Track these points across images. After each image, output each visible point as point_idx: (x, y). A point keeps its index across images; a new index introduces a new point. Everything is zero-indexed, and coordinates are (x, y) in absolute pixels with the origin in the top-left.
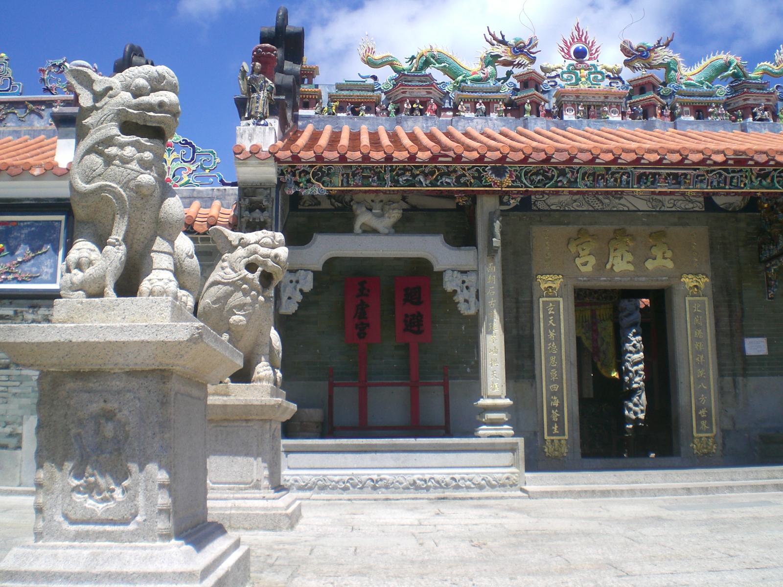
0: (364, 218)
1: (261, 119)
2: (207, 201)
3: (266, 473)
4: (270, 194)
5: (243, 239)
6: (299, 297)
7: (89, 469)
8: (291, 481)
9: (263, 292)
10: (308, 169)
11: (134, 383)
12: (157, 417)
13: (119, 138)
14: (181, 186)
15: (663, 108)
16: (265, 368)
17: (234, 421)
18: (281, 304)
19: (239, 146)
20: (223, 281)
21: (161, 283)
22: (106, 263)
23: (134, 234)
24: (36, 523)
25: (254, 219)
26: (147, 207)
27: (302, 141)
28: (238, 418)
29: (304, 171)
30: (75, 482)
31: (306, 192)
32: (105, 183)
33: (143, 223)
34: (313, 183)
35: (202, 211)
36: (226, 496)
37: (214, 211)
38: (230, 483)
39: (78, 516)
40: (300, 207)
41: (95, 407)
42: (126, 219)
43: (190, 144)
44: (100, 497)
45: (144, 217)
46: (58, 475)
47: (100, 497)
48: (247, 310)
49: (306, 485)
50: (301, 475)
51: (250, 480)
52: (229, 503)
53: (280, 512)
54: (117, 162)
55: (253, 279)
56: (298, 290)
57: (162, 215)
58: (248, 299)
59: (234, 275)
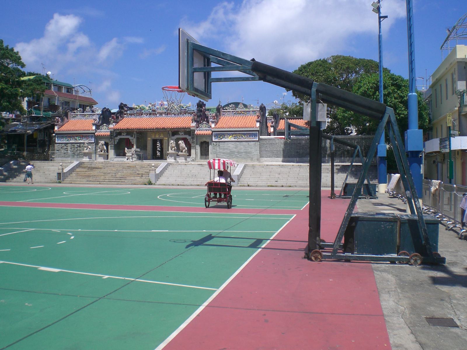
0: (122, 134)
15: (170, 114)
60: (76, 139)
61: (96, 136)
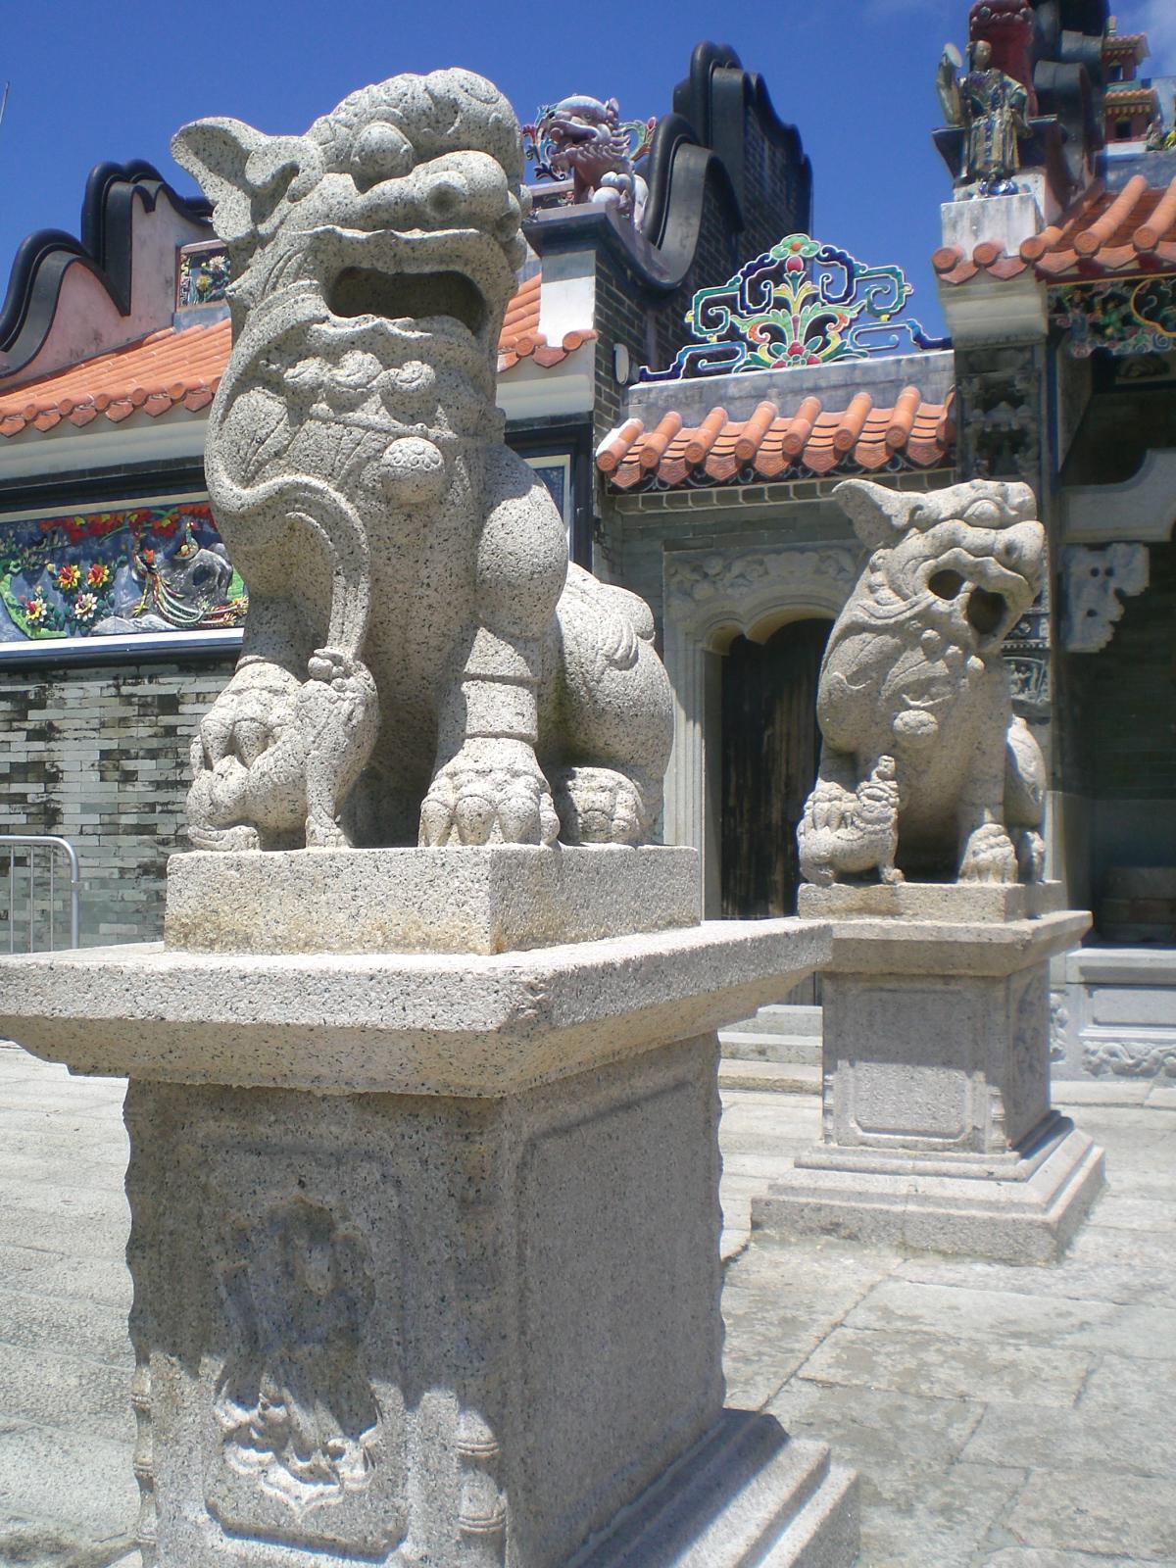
1: (999, 179)
2: (886, 390)
3: (997, 1110)
4: (1031, 362)
5: (920, 508)
6: (1114, 611)
7: (268, 1385)
8: (1101, 1054)
9: (980, 644)
10: (1124, 291)
11: (380, 1134)
12: (450, 1245)
13: (324, 327)
14: (825, 360)
16: (993, 840)
17: (913, 977)
18: (1070, 630)
19: (949, 250)
20: (873, 621)
21: (481, 786)
22: (304, 738)
23: (404, 629)
24: (142, 1517)
25: (996, 426)
26: (432, 540)
27: (1106, 223)
28: (923, 971)
29: (1112, 297)
30: (240, 1415)
31: (1127, 348)
32: (305, 479)
33: (421, 591)
34: (1138, 326)
35: (877, 415)
36: (895, 1163)
37: (900, 415)
38: (905, 1132)
39: (244, 1517)
40: (1119, 381)
41: (279, 1197)
42: (364, 586)
43: (840, 258)
44: (305, 1465)
45: (424, 573)
46: (188, 1387)
47: (305, 1465)
48: (938, 695)
49: (1137, 1065)
50: (1125, 1039)
51: (955, 1127)
52: (903, 1185)
53: (1029, 1216)
54: (321, 407)
55: (950, 615)
56: (1111, 592)
57: (485, 558)
58: (940, 668)
59: (901, 605)
60: (203, 574)
61: (624, 480)
